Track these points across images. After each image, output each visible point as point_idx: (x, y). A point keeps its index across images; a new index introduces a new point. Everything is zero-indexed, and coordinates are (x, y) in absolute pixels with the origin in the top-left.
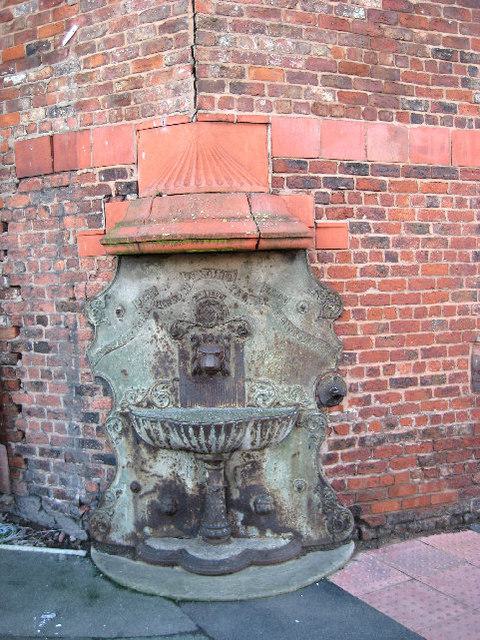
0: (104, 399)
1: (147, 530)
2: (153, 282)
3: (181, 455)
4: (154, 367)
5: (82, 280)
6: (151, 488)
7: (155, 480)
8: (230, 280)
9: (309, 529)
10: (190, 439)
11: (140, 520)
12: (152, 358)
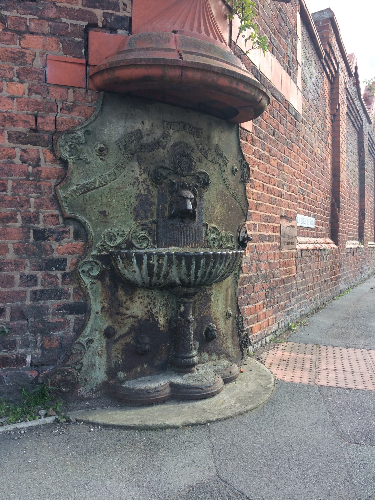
0: (75, 243)
1: (121, 375)
2: (139, 126)
3: (156, 293)
4: (135, 209)
5: (51, 110)
6: (126, 329)
7: (130, 322)
8: (198, 137)
12: (133, 200)
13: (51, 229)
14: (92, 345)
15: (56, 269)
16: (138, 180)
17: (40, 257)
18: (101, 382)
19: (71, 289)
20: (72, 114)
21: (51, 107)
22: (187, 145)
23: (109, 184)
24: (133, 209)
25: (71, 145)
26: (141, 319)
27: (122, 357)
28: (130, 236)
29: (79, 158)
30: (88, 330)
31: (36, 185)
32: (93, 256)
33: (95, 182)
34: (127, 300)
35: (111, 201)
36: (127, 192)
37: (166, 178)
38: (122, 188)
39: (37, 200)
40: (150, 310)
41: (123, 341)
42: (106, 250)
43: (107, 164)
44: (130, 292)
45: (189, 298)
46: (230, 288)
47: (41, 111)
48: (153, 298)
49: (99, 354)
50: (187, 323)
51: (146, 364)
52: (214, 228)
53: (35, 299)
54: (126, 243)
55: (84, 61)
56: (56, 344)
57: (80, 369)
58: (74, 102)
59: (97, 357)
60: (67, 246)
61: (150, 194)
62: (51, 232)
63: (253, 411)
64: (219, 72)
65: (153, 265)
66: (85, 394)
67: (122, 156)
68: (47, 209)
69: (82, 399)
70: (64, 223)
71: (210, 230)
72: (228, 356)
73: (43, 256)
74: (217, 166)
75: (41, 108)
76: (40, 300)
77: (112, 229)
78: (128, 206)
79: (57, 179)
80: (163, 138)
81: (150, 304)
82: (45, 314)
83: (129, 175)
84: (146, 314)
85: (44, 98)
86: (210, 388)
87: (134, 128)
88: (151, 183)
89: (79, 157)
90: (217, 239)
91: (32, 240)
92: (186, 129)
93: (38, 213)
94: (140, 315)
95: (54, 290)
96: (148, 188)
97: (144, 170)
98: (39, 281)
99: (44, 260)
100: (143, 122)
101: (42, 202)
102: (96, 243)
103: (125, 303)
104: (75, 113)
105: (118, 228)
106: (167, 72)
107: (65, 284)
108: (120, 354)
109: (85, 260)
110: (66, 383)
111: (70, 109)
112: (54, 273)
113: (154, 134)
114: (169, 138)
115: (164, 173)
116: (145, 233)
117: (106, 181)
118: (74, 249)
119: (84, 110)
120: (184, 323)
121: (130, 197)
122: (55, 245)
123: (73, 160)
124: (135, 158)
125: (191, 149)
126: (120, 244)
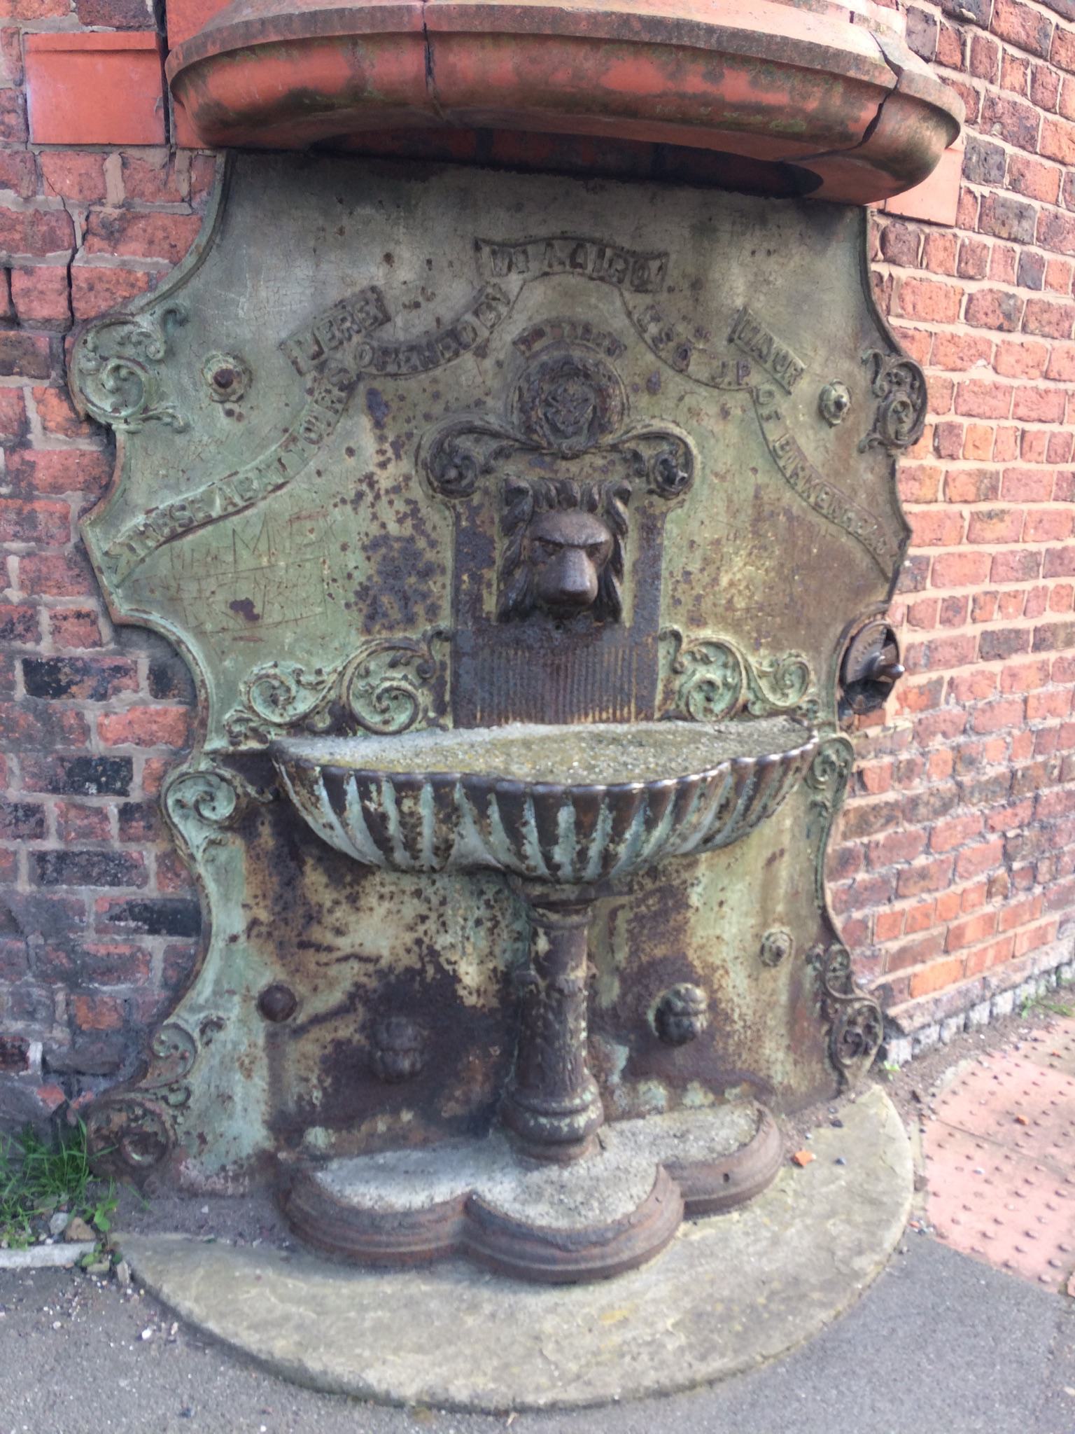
0: (156, 706)
1: (318, 1137)
2: (372, 273)
4: (363, 592)
5: (51, 243)
6: (336, 997)
7: (350, 974)
8: (641, 288)
9: (789, 1067)
10: (548, 837)
11: (291, 1106)
12: (354, 559)
13: (77, 659)
14: (220, 1036)
15: (99, 791)
16: (371, 485)
17: (48, 750)
18: (250, 1151)
19: (149, 854)
20: (121, 248)
21: (52, 230)
22: (587, 329)
23: (262, 505)
24: (357, 593)
25: (117, 368)
26: (391, 969)
27: (320, 1081)
28: (344, 690)
29: (147, 416)
30: (204, 989)
31: (19, 512)
32: (214, 755)
33: (207, 500)
34: (337, 903)
35: (272, 566)
36: (329, 533)
37: (487, 471)
38: (310, 517)
39: (26, 561)
40: (426, 940)
41: (325, 1034)
42: (257, 734)
43: (250, 432)
44: (348, 879)
45: (567, 913)
46: (786, 858)
47: (17, 249)
48: (435, 900)
49: (242, 1065)
50: (556, 995)
51: (410, 1107)
52: (708, 643)
53: (42, 877)
54: (331, 713)
55: (149, 40)
56: (110, 1020)
57: (183, 1106)
58: (126, 205)
59: (238, 1076)
60: (130, 716)
61: (423, 533)
62: (77, 671)
63: (720, 1388)
64: (602, 34)
65: (384, 817)
66: (201, 1179)
67: (309, 399)
68: (61, 594)
69: (192, 1193)
70: (117, 638)
71: (692, 653)
72: (761, 1089)
73: (59, 747)
74: (737, 402)
75: (17, 236)
76: (56, 881)
77: (276, 666)
78: (334, 580)
79: (87, 488)
80: (476, 313)
81: (423, 919)
82: (72, 928)
83: (336, 469)
84: (408, 951)
85: (27, 199)
86: (596, 1251)
87: (353, 284)
88: (427, 496)
89: (146, 409)
90: (726, 684)
91: (20, 692)
92: (581, 266)
93: (33, 605)
94: (385, 953)
95: (97, 854)
96: (415, 512)
97: (397, 446)
98: (52, 822)
99: (62, 759)
100: (388, 258)
101: (44, 570)
102: (222, 711)
103: (330, 911)
104: (133, 246)
105: (298, 660)
106: (366, 65)
107: (130, 839)
108: (317, 1072)
109: (184, 768)
110: (144, 1142)
111: (114, 234)
112: (95, 801)
113: (438, 299)
114: (503, 310)
115: (479, 451)
116: (405, 678)
117: (248, 495)
118: (155, 727)
119: (164, 229)
120: (548, 995)
121: (344, 548)
122: (93, 712)
123: (126, 422)
124: (360, 399)
125: (606, 343)
126: (306, 716)
